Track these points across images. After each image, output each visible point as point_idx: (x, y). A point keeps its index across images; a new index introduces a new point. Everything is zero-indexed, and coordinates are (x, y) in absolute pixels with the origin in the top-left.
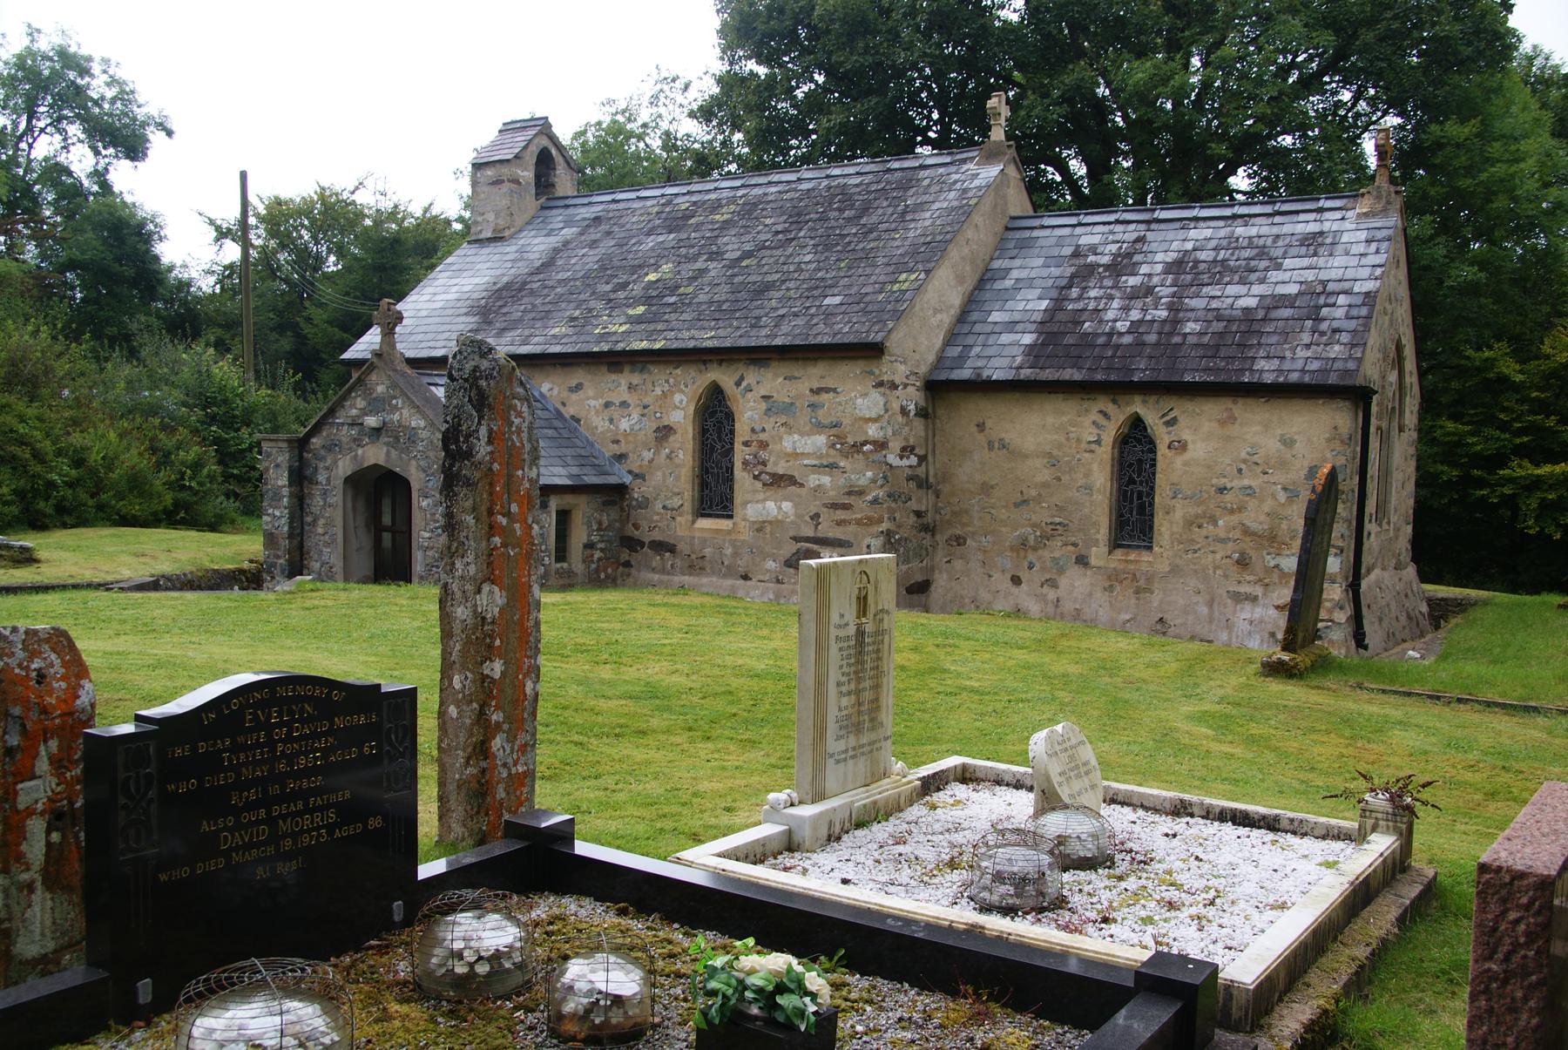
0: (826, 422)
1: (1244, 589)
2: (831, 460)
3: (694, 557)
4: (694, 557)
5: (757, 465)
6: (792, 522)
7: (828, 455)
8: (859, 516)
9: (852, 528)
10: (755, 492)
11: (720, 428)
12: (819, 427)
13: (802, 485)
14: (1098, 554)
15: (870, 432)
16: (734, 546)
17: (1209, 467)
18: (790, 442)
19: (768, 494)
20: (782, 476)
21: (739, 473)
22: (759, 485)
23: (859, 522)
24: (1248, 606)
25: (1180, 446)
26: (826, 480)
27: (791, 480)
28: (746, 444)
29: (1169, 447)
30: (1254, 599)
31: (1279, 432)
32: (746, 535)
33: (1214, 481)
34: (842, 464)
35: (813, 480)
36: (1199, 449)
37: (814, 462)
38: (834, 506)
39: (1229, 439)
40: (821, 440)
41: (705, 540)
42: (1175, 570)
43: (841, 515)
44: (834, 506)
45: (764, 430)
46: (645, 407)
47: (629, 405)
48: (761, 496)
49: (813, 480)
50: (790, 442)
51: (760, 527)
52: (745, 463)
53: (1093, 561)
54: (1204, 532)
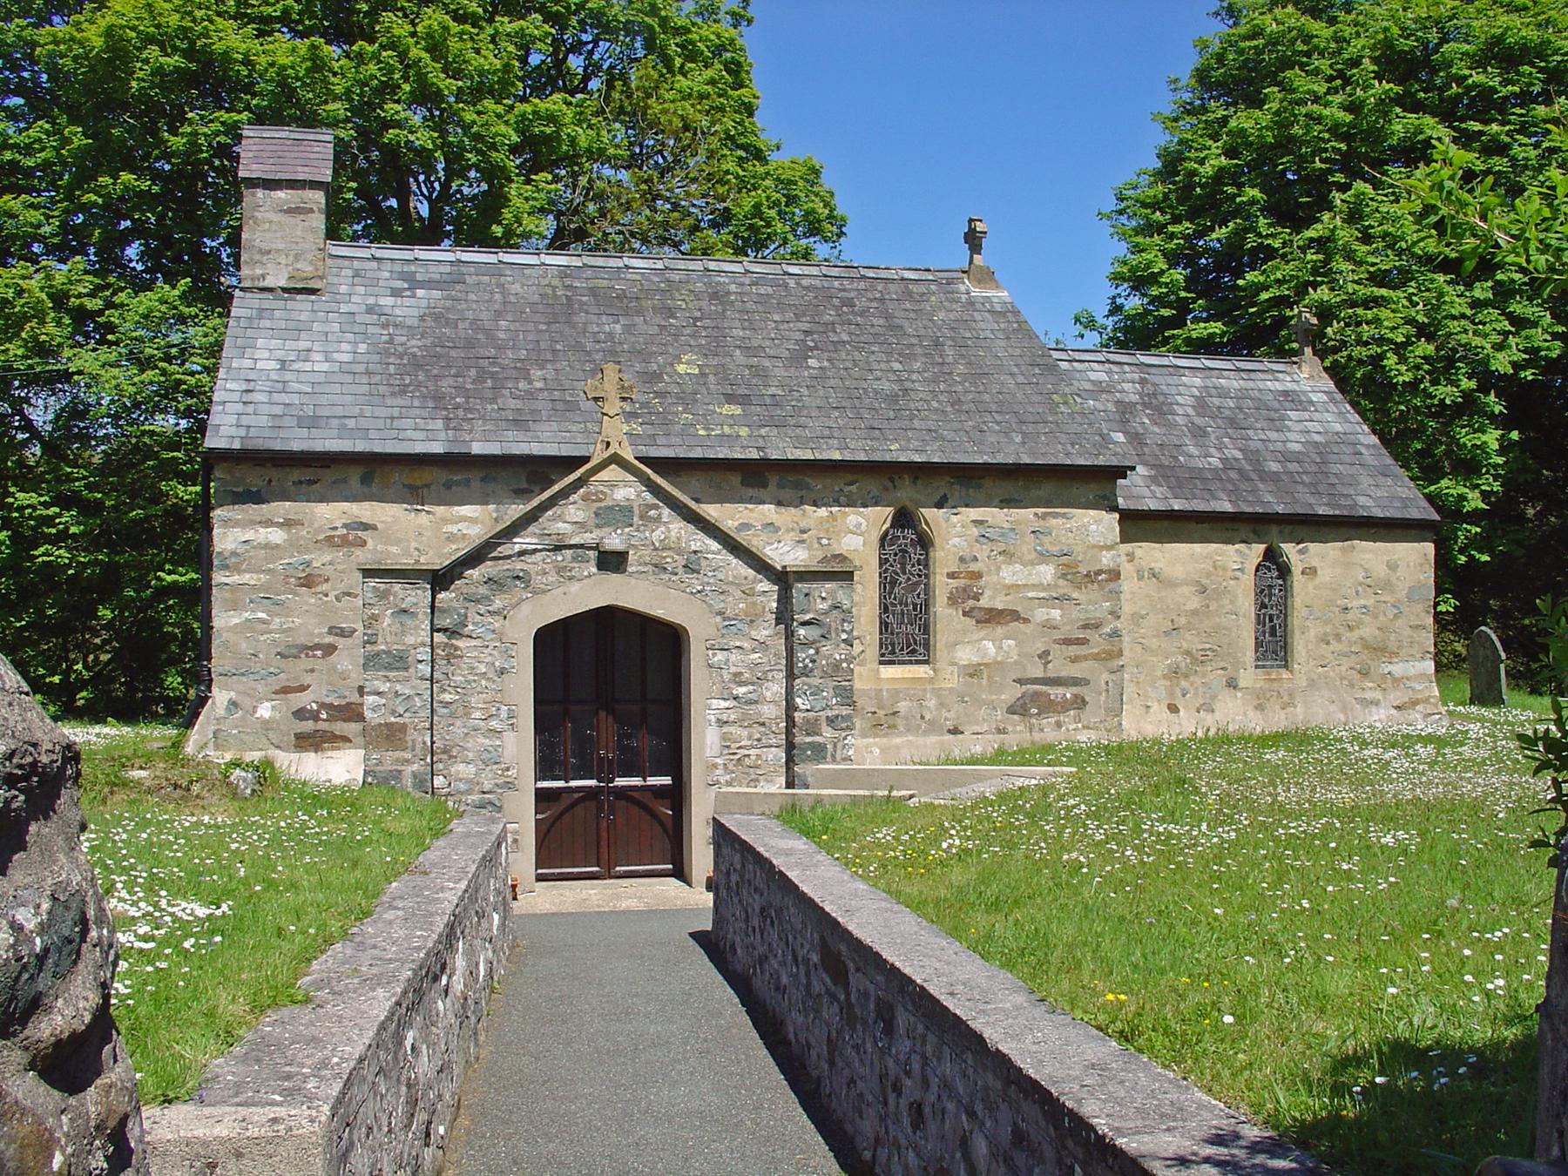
0: (1055, 550)
1: (1369, 695)
2: (1062, 591)
3: (881, 713)
4: (881, 713)
5: (964, 597)
6: (1016, 663)
7: (1056, 586)
8: (1096, 651)
9: (1084, 664)
10: (965, 632)
11: (904, 557)
12: (1044, 557)
13: (1026, 621)
14: (1249, 677)
15: (1105, 561)
16: (939, 697)
17: (1333, 590)
18: (1010, 574)
19: (983, 633)
20: (1002, 611)
21: (941, 608)
22: (970, 622)
23: (1096, 657)
24: (1374, 709)
25: (1310, 572)
26: (1056, 614)
27: (1014, 616)
28: (951, 575)
29: (1303, 573)
30: (1377, 703)
31: (1386, 558)
32: (951, 680)
33: (1339, 602)
34: (1075, 595)
35: (1041, 614)
36: (1325, 575)
37: (1042, 595)
38: (1068, 642)
39: (1348, 565)
40: (1047, 572)
41: (897, 692)
42: (1312, 684)
43: (1074, 650)
44: (1068, 642)
45: (975, 559)
46: (803, 532)
47: (777, 529)
48: (975, 637)
49: (1041, 614)
50: (1010, 574)
51: (974, 671)
52: (953, 600)
53: (1242, 684)
54: (1331, 648)
